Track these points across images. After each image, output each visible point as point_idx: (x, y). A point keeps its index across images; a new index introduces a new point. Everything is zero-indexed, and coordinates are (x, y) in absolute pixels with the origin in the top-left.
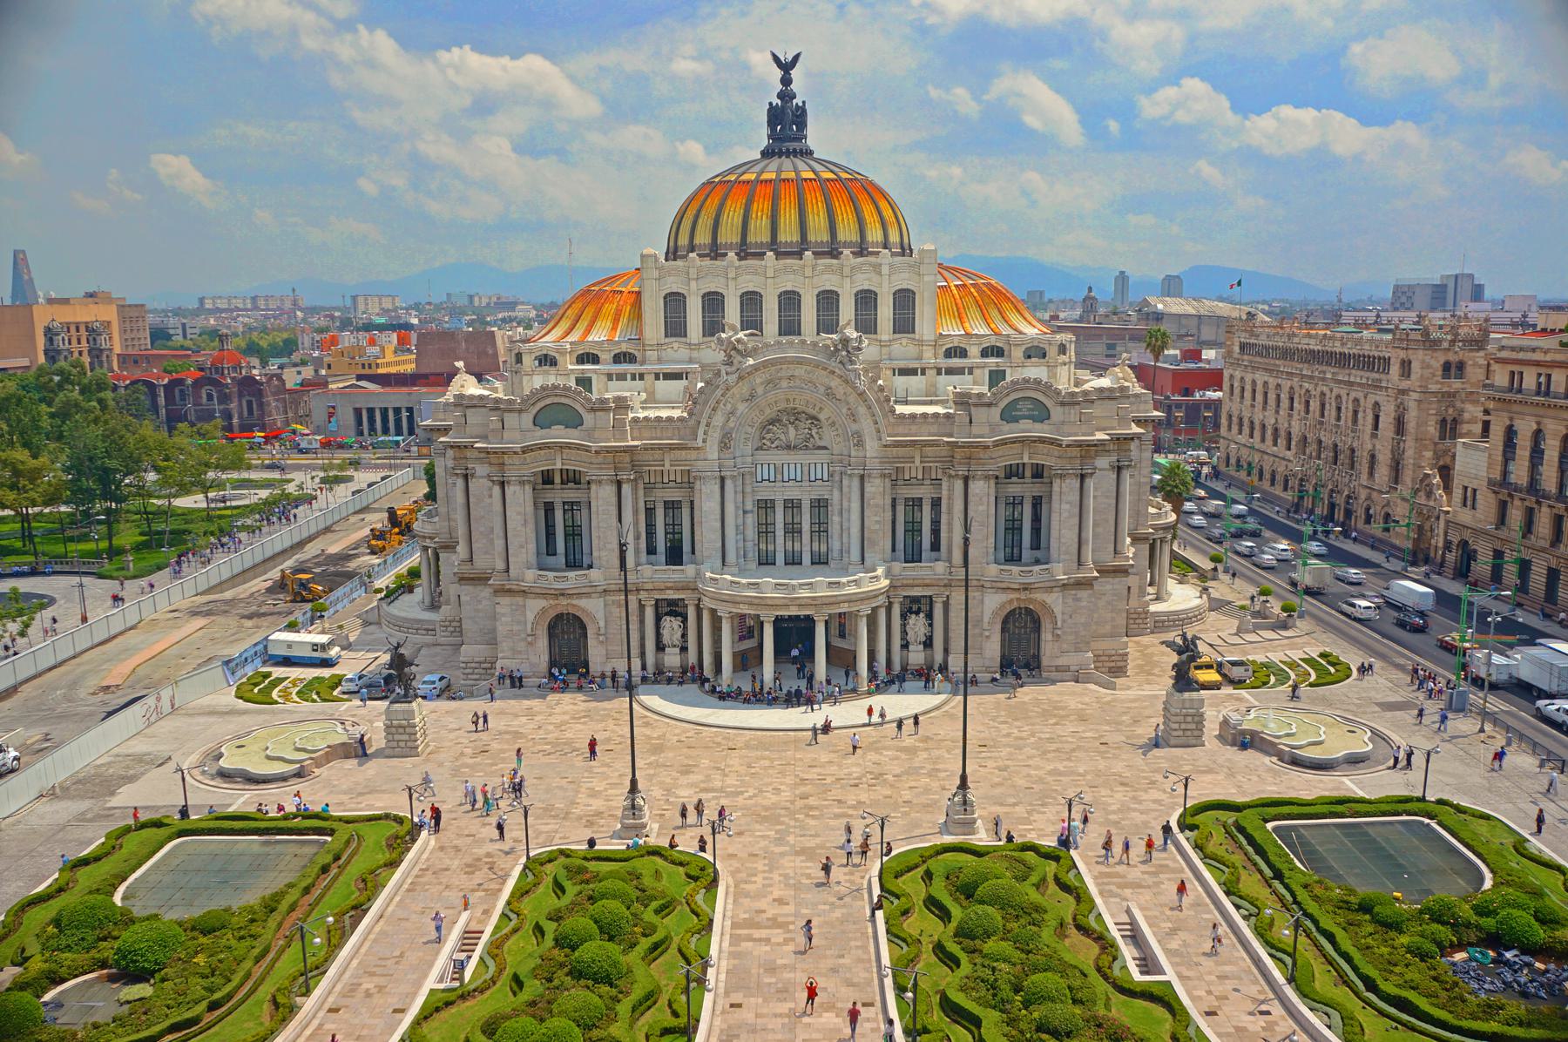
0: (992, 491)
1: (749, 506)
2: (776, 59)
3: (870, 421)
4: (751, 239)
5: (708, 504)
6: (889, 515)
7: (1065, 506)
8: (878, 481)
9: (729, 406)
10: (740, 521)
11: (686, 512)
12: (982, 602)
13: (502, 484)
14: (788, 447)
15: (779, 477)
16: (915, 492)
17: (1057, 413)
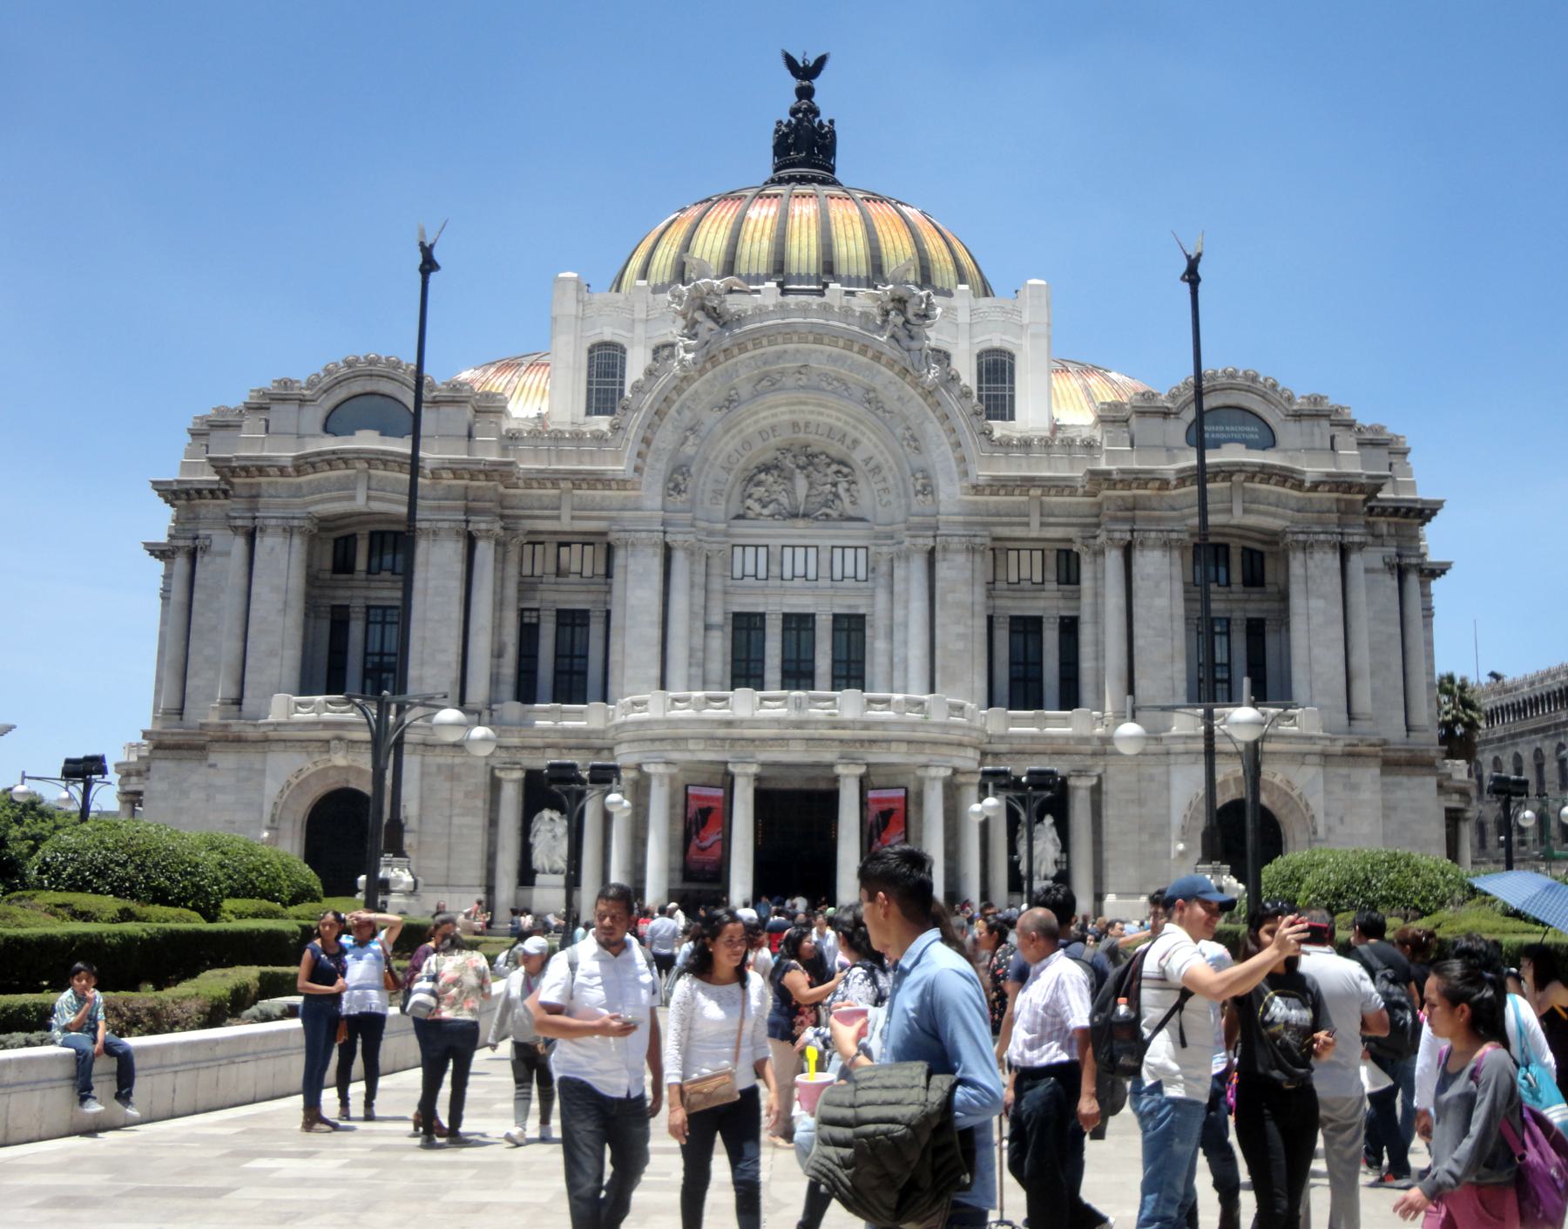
0: (1177, 571)
1: (717, 617)
2: (790, 62)
3: (947, 448)
4: (742, 267)
5: (637, 592)
6: (981, 624)
7: (1316, 604)
8: (961, 559)
9: (687, 414)
10: (698, 641)
11: (596, 629)
12: (1168, 786)
13: (251, 536)
14: (795, 516)
15: (775, 570)
16: (1029, 608)
17: (1288, 433)
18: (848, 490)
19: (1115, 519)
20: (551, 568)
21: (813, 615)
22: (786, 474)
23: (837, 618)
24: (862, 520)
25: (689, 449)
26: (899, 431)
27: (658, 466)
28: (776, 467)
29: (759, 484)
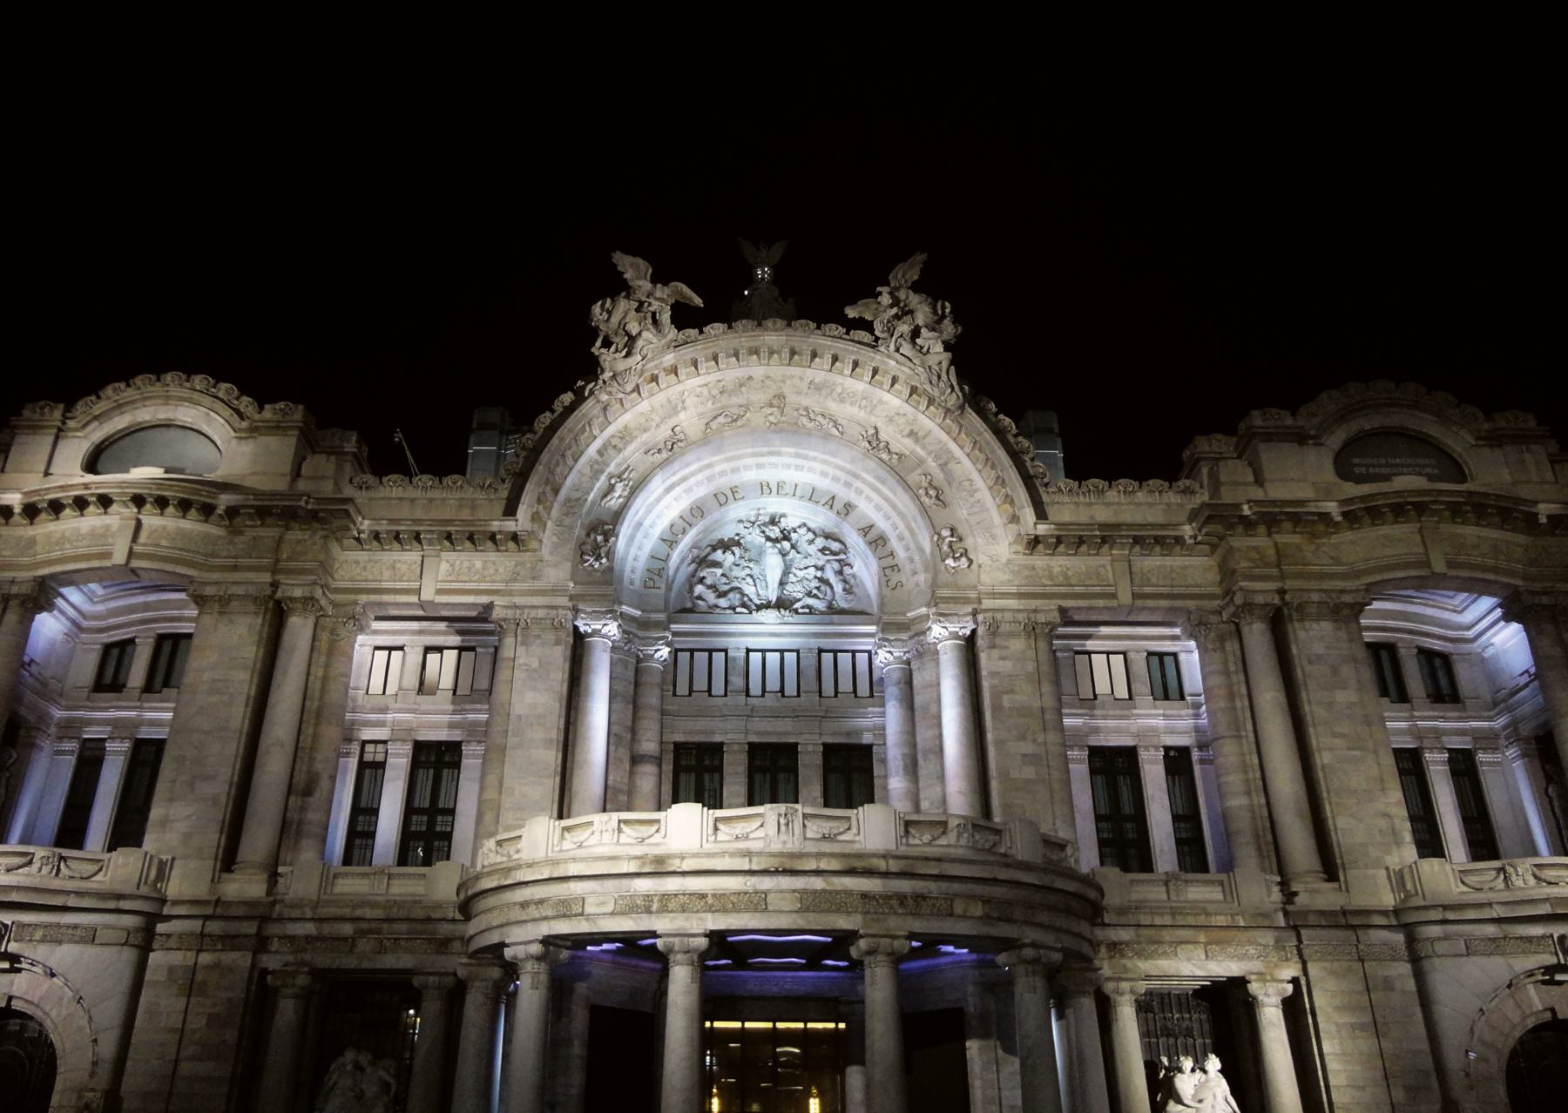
1: (649, 745)
8: (1018, 645)
15: (737, 681)
16: (1114, 732)
18: (840, 573)
19: (1253, 578)
20: (412, 681)
21: (796, 744)
22: (752, 554)
23: (829, 750)
24: (862, 613)
25: (614, 502)
26: (914, 477)
27: (567, 521)
28: (738, 544)
29: (717, 564)
